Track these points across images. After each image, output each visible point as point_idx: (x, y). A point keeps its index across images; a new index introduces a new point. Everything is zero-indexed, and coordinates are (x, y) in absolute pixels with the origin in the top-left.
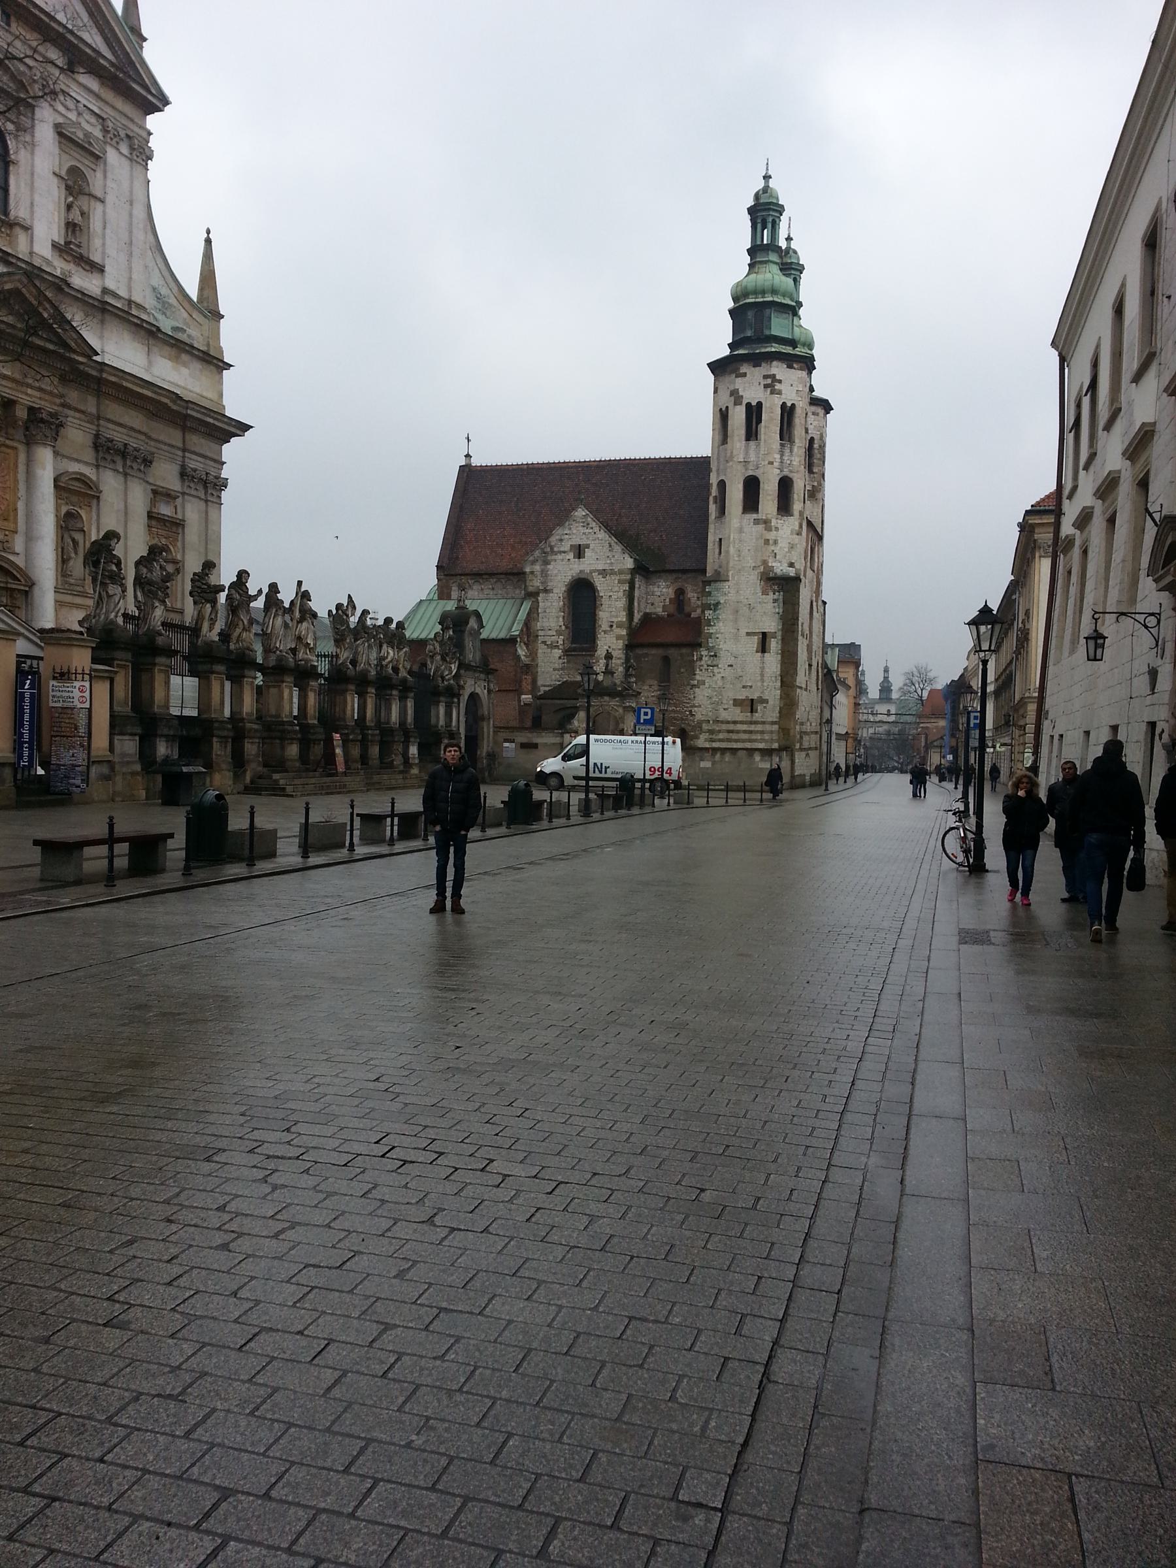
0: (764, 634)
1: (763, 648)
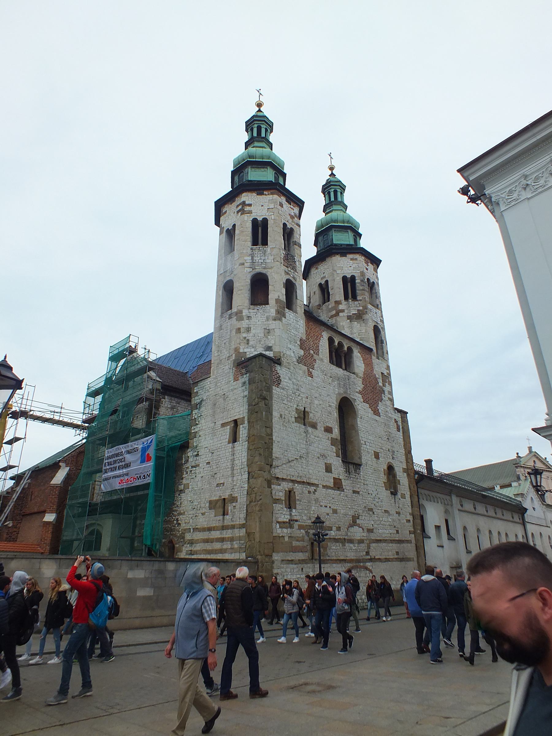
0: (235, 421)
1: (234, 439)
